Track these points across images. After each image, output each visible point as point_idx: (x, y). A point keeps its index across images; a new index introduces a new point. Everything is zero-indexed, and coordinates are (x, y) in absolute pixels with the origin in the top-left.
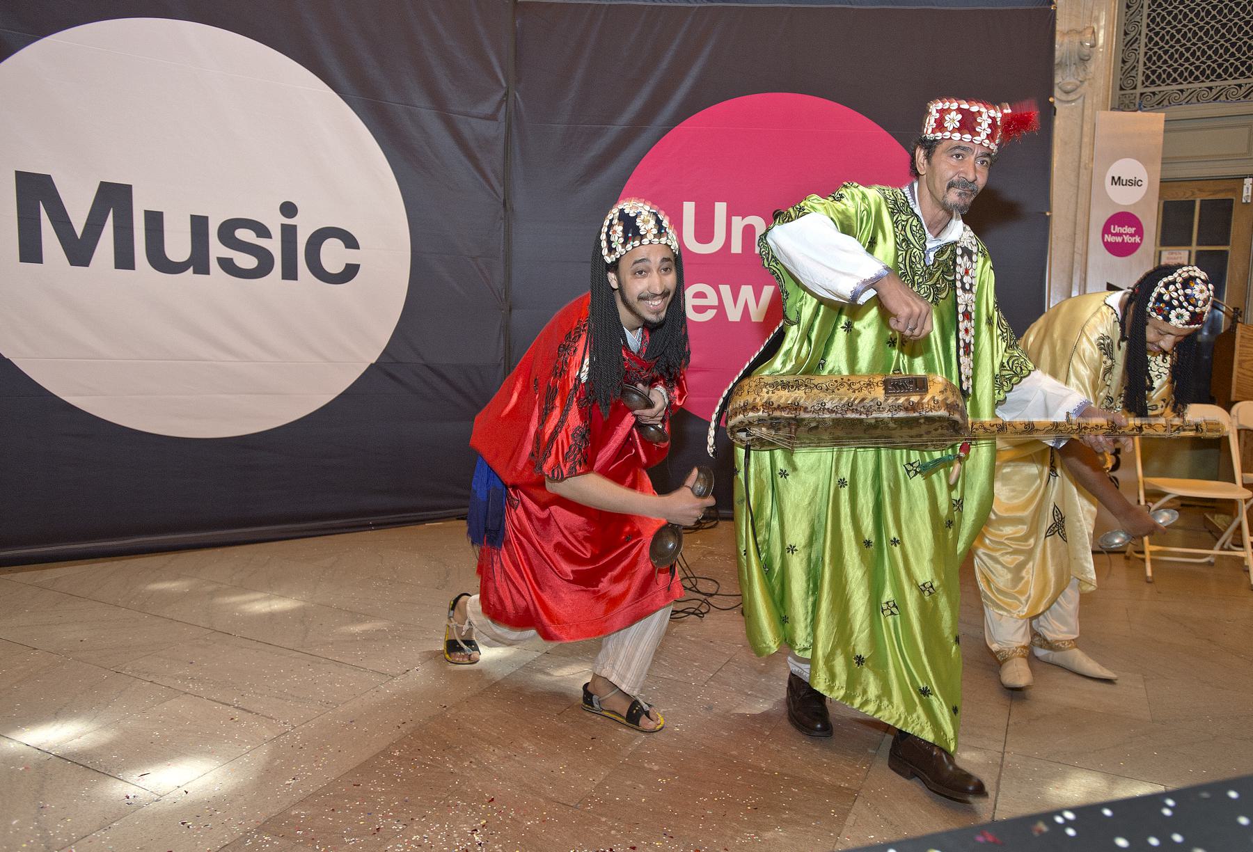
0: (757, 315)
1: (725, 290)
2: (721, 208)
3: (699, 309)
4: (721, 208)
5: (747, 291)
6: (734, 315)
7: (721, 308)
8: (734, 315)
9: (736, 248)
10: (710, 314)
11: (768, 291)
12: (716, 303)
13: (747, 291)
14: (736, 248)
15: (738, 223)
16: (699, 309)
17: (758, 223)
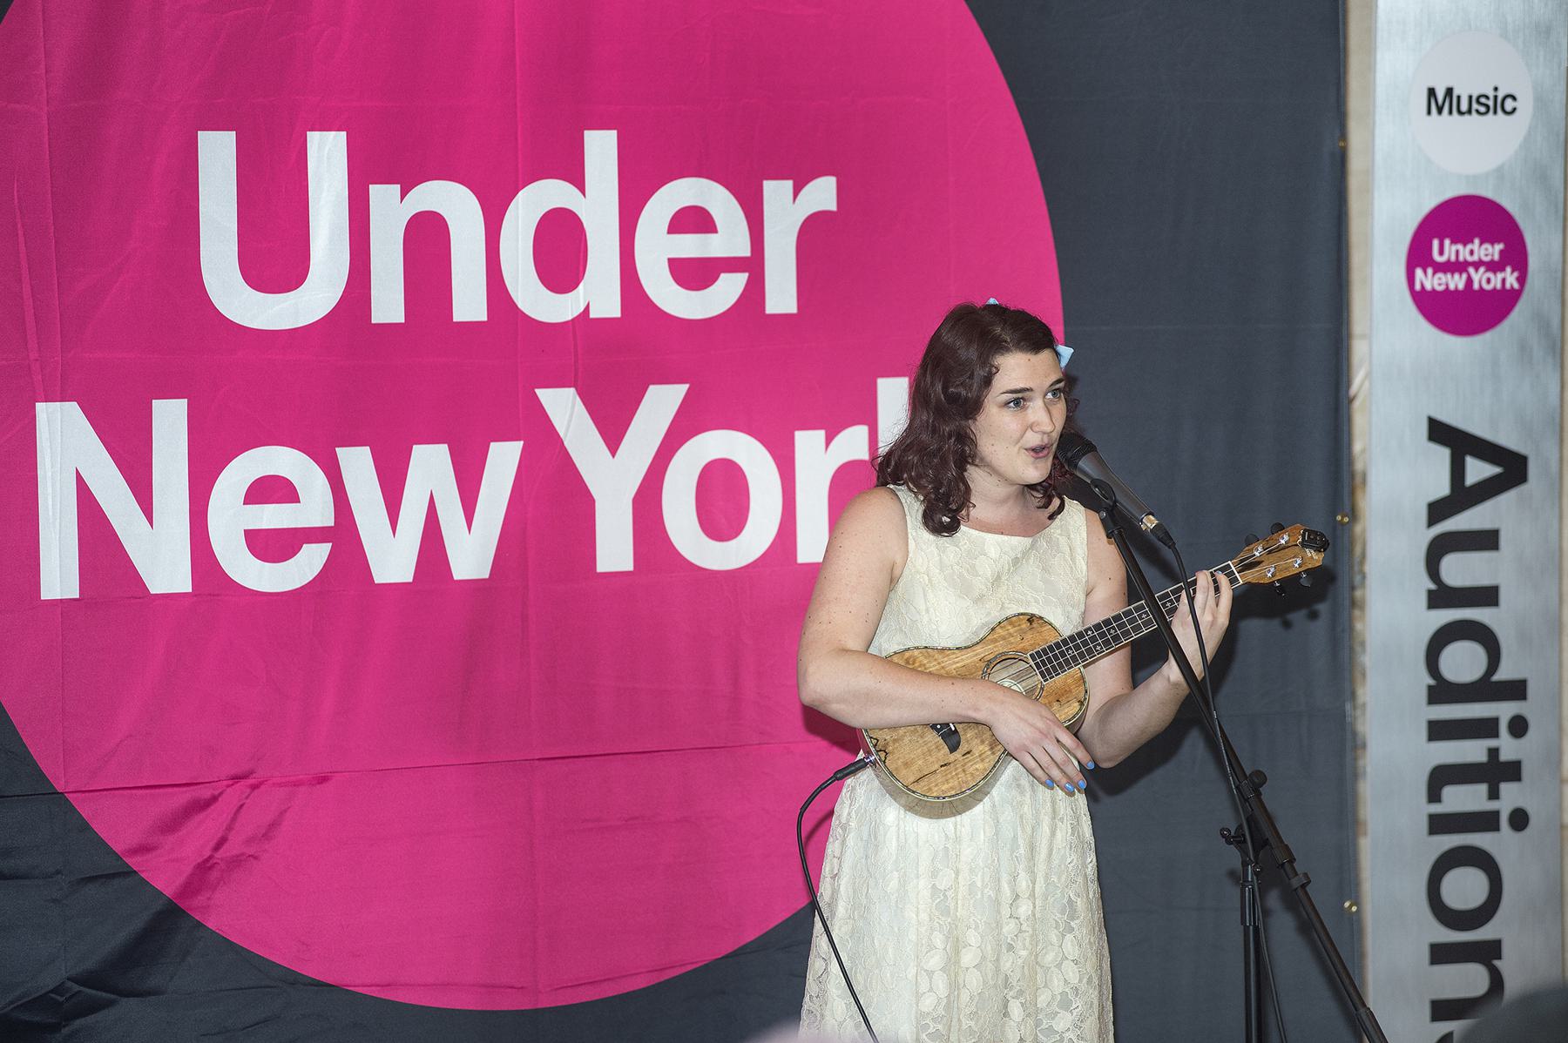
0: (471, 555)
1: (357, 462)
2: (327, 155)
3: (272, 546)
4: (327, 155)
5: (430, 466)
6: (392, 559)
7: (342, 534)
8: (392, 559)
9: (388, 305)
10: (310, 561)
11: (503, 459)
12: (329, 521)
13: (430, 466)
14: (388, 305)
15: (391, 209)
16: (272, 546)
17: (454, 202)
